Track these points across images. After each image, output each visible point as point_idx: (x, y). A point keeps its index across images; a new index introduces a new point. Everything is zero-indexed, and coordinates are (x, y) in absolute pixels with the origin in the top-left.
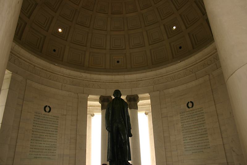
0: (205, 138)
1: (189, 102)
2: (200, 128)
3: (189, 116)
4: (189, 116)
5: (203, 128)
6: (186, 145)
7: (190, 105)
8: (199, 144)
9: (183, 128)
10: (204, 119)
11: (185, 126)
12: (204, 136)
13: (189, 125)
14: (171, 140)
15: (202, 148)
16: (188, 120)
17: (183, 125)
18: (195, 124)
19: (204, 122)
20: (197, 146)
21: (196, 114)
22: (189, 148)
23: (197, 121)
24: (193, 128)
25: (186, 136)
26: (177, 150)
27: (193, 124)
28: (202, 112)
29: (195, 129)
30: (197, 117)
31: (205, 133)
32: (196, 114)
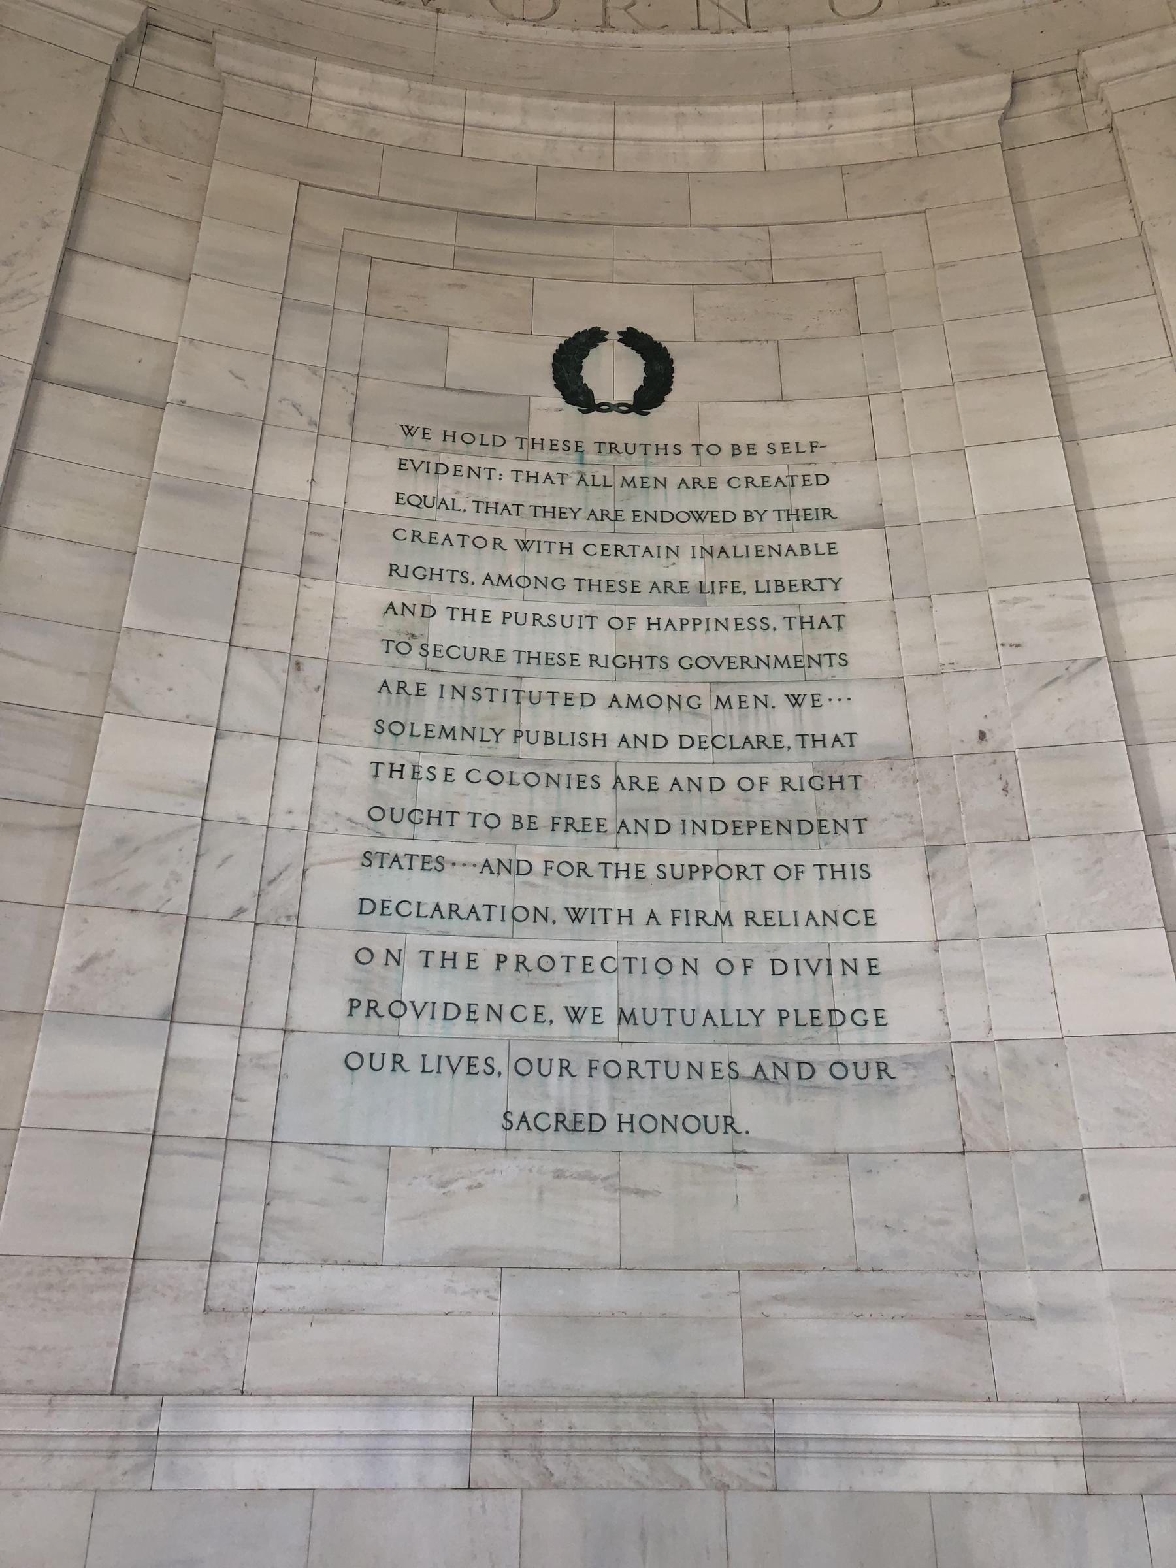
0: (816, 895)
1: (595, 337)
2: (726, 723)
3: (559, 513)
4: (559, 513)
5: (784, 721)
6: (394, 958)
7: (613, 373)
8: (663, 967)
9: (415, 659)
10: (812, 604)
11: (440, 631)
12: (808, 852)
13: (536, 640)
14: (97, 792)
15: (723, 1055)
16: (538, 565)
17: (428, 612)
18: (641, 640)
19: (826, 642)
20: (626, 1017)
21: (699, 517)
22: (450, 1012)
23: (689, 613)
24: (588, 700)
25: (431, 795)
26: (170, 1016)
27: (604, 642)
28: (803, 499)
29: (640, 723)
30: (707, 552)
31: (810, 804)
32: (699, 517)
